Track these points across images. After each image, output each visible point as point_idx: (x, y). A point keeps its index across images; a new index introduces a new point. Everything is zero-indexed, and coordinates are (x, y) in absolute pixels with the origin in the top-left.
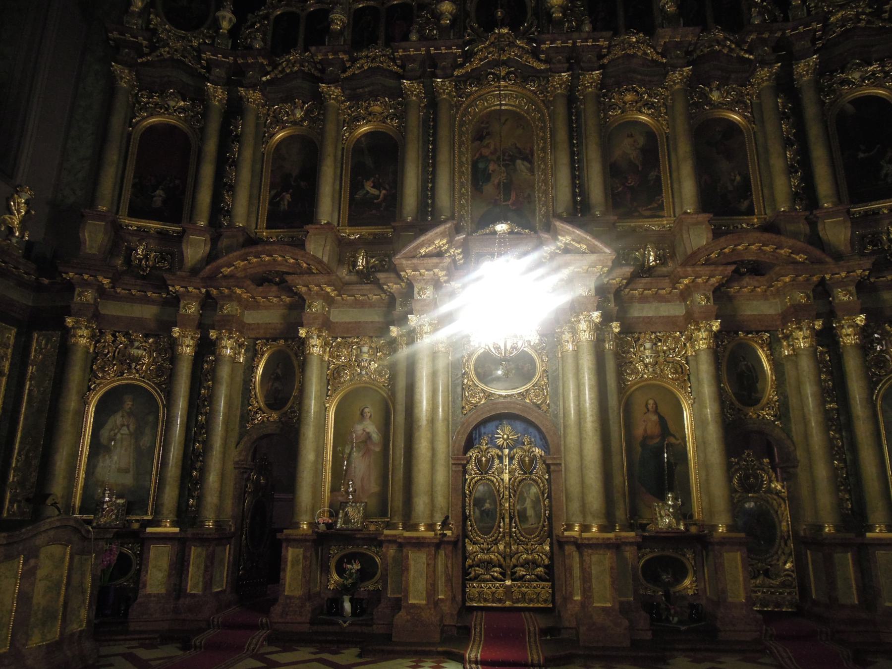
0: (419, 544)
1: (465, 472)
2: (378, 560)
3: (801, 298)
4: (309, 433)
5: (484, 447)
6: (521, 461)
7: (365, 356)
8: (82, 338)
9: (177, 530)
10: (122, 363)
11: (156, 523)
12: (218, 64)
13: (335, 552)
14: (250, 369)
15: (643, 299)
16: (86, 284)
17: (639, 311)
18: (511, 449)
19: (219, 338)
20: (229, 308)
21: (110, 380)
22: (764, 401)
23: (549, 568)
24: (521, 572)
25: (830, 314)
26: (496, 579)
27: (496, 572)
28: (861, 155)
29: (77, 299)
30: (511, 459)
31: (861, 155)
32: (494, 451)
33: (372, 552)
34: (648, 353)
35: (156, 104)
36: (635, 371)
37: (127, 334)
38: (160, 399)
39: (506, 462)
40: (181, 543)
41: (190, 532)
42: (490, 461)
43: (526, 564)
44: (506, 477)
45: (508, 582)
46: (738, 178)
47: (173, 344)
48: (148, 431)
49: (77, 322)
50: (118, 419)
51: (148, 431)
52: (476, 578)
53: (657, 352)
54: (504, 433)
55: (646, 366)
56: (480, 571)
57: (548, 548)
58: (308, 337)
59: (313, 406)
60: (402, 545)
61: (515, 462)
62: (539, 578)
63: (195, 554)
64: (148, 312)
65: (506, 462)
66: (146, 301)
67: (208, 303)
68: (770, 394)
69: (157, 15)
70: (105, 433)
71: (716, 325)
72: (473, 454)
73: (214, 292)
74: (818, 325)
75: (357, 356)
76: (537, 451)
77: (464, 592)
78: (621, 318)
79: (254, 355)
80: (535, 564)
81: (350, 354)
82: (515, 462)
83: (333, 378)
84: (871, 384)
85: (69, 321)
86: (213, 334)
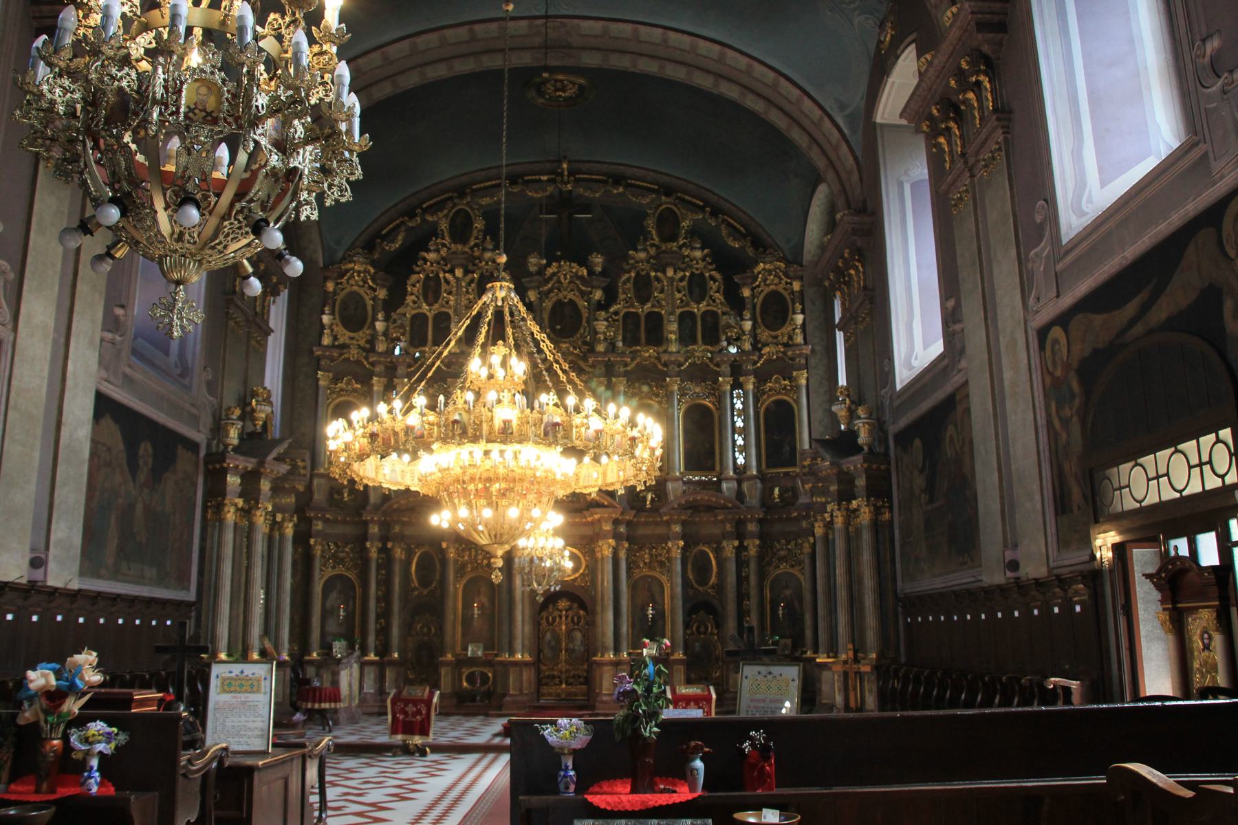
0: (516, 664)
1: (539, 624)
2: (490, 675)
3: (728, 527)
4: (450, 604)
5: (551, 610)
6: (572, 620)
7: (480, 557)
8: (318, 551)
9: (377, 658)
10: (334, 561)
11: (367, 655)
12: (380, 363)
13: (466, 672)
14: (410, 564)
15: (646, 524)
16: (317, 518)
17: (641, 531)
18: (567, 611)
19: (393, 547)
20: (397, 529)
21: (329, 572)
22: (711, 583)
23: (586, 679)
24: (571, 680)
25: (740, 535)
26: (556, 685)
27: (557, 681)
28: (776, 437)
29: (314, 528)
30: (567, 617)
31: (776, 437)
32: (556, 613)
33: (486, 670)
34: (647, 556)
35: (342, 390)
36: (638, 567)
37: (336, 544)
38: (356, 583)
39: (564, 619)
40: (381, 666)
41: (386, 659)
42: (554, 619)
43: (573, 677)
44: (564, 627)
45: (564, 686)
46: (707, 446)
47: (364, 551)
48: (351, 603)
49: (316, 542)
50: (334, 596)
51: (351, 603)
52: (546, 684)
53: (651, 555)
54: (563, 604)
55: (645, 563)
56: (547, 680)
57: (586, 667)
58: (448, 548)
59: (451, 588)
60: (505, 664)
61: (569, 619)
62: (581, 684)
63: (389, 674)
64: (348, 530)
65: (564, 619)
66: (344, 522)
67: (385, 526)
68: (713, 580)
69: (337, 325)
70: (328, 604)
71: (681, 543)
72: (544, 614)
73: (388, 519)
74: (736, 543)
75: (475, 556)
76: (582, 612)
77: (538, 692)
78: (628, 540)
79: (410, 554)
80: (579, 677)
81: (470, 556)
82: (569, 619)
83: (461, 570)
84: (762, 576)
85: (312, 541)
86: (390, 545)
